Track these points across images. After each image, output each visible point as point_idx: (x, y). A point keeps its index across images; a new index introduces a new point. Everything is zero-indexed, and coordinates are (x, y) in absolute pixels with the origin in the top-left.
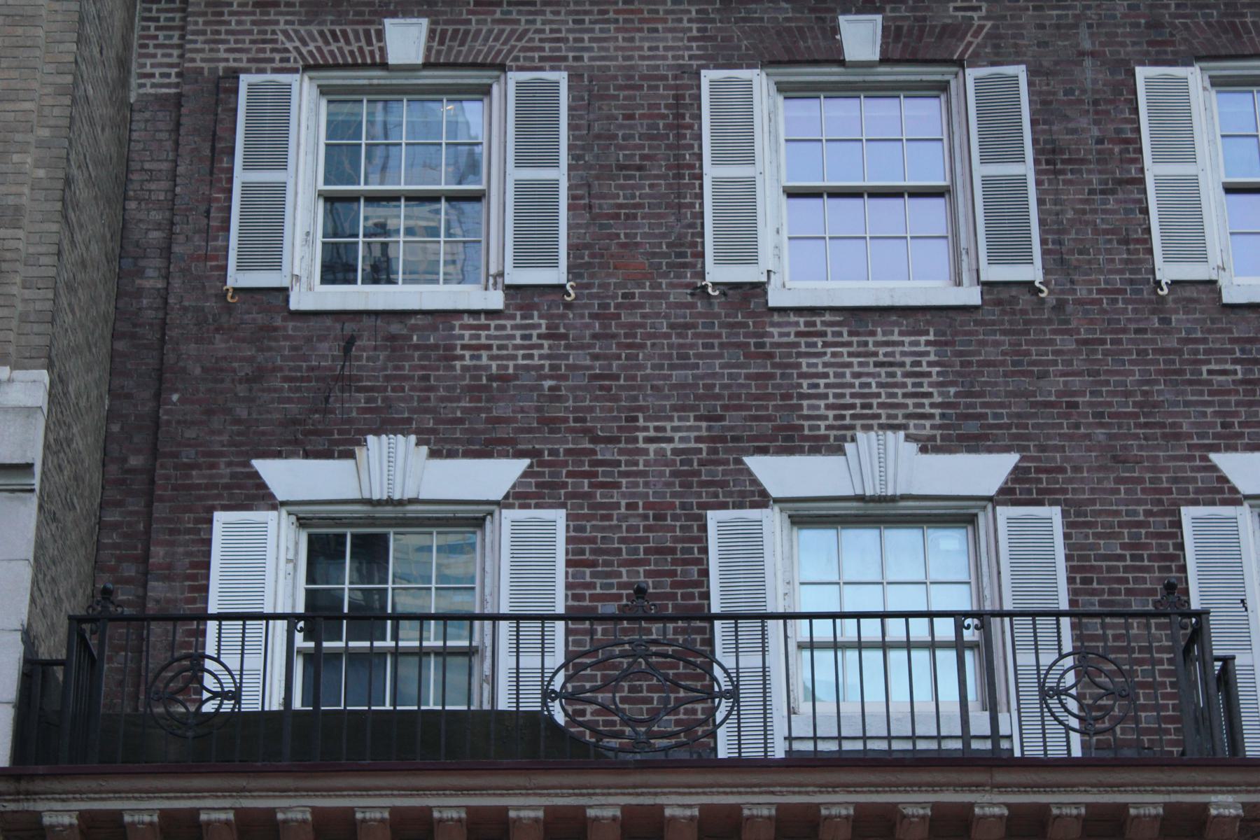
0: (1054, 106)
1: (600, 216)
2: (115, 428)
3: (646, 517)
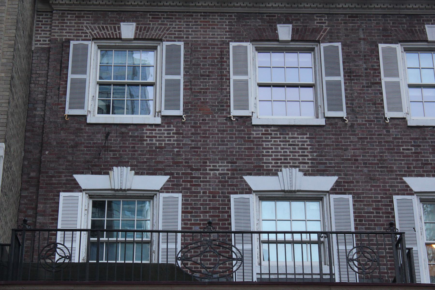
1: (194, 92)
2: (26, 163)
3: (209, 197)
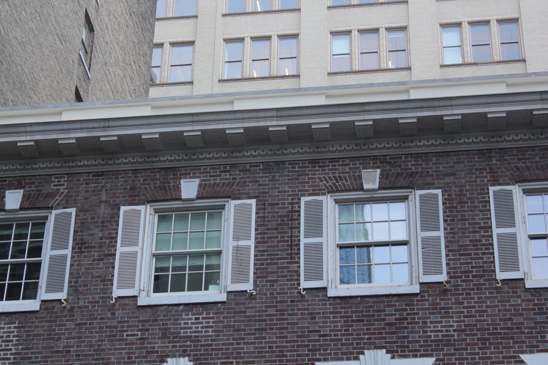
0: (86, 224)
